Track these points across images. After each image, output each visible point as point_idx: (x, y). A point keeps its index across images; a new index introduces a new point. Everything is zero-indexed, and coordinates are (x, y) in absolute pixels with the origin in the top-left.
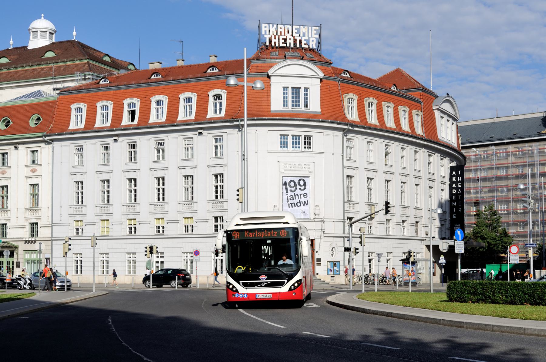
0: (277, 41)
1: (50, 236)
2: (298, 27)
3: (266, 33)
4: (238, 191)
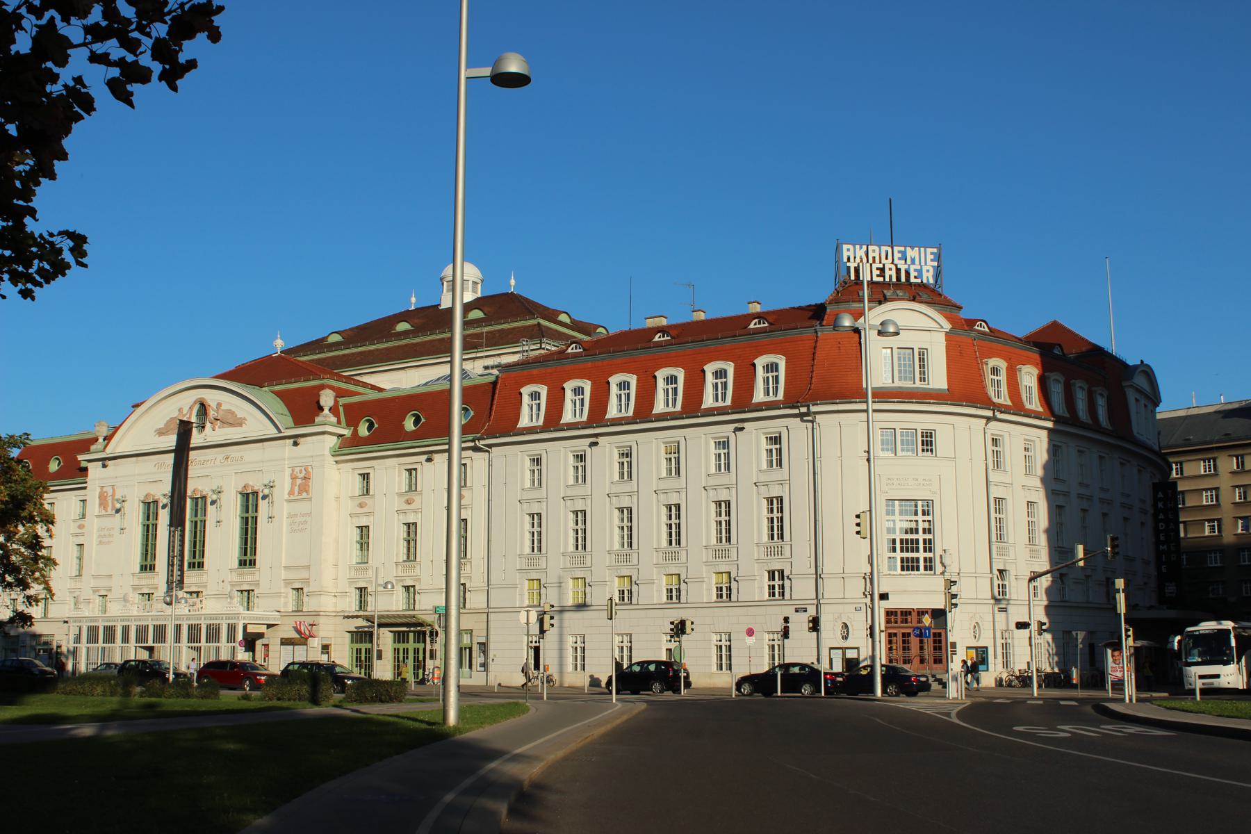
1: (1185, 465)
2: (902, 249)
3: (849, 259)
4: (858, 516)
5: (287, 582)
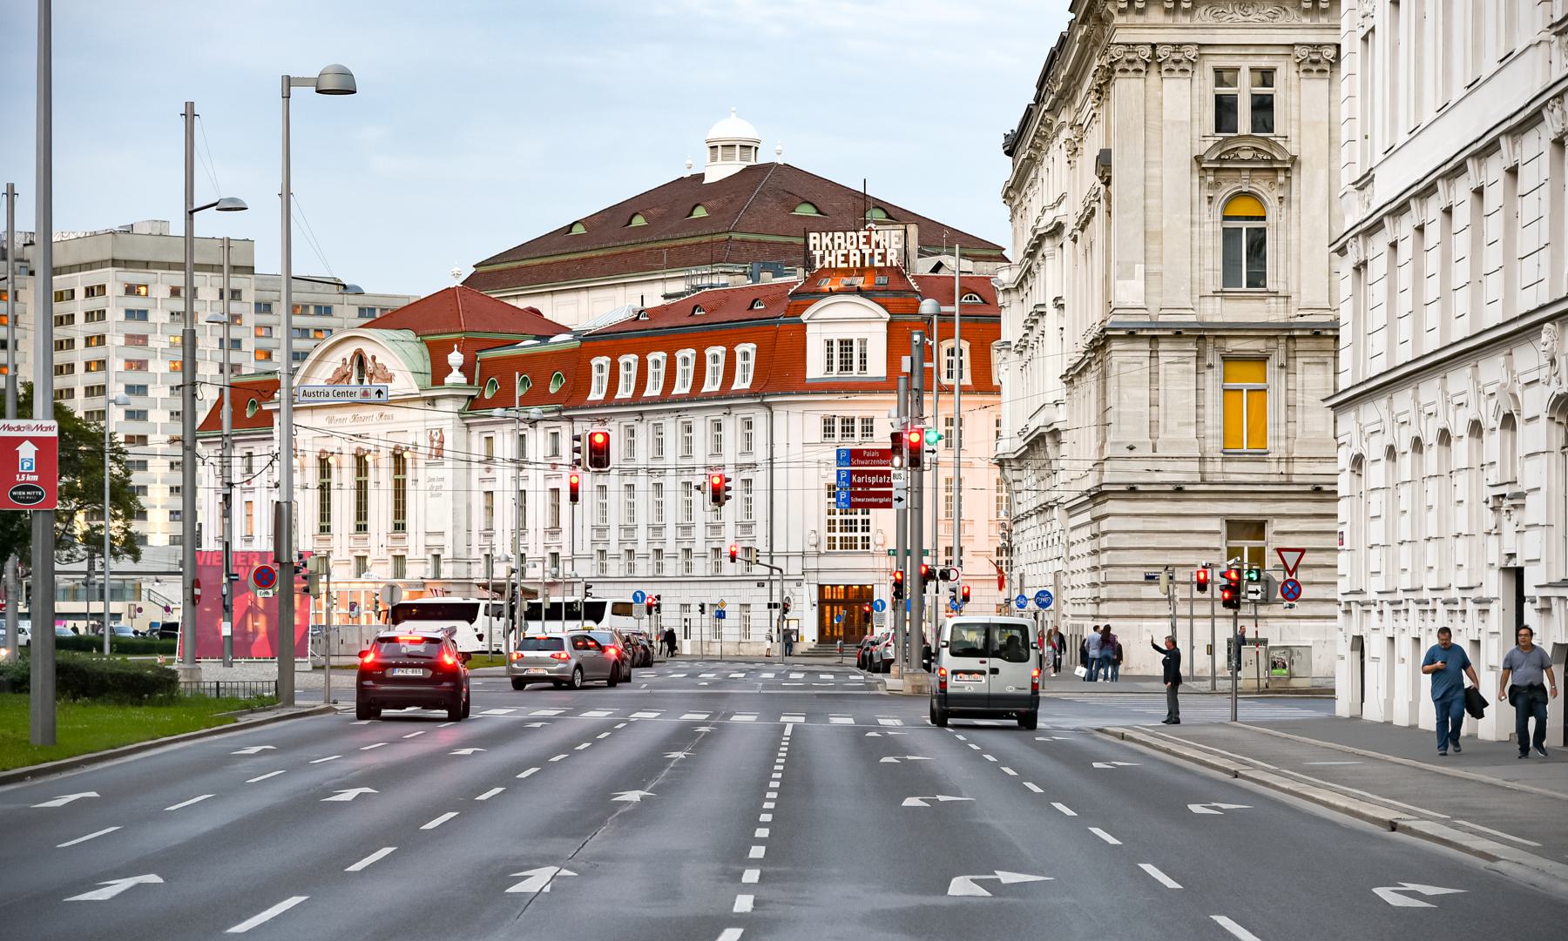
0: (833, 259)
5: (428, 548)
